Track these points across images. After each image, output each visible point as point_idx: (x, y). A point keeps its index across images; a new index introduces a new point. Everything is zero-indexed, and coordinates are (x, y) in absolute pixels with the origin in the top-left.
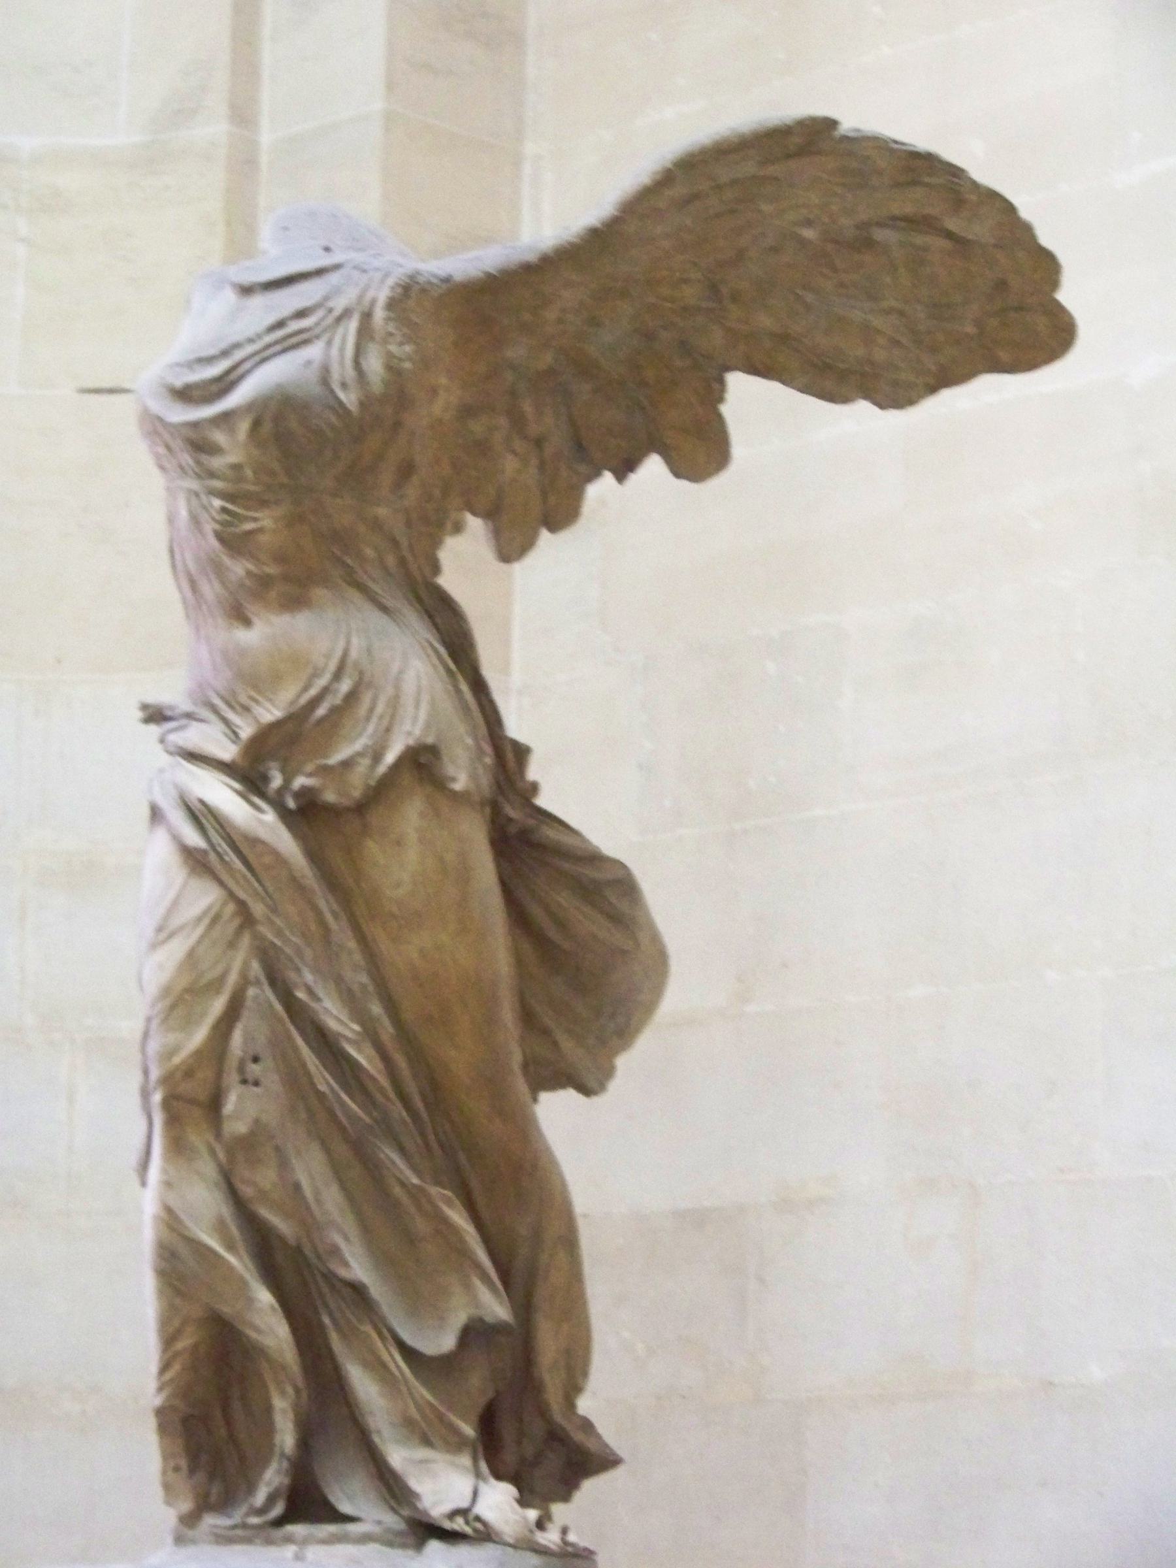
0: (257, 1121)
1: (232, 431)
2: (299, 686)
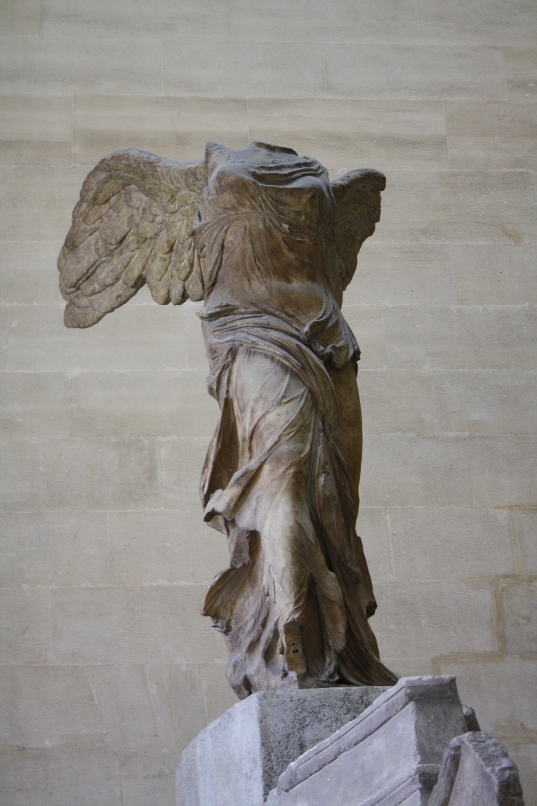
0: (330, 491)
1: (300, 198)
2: (323, 311)
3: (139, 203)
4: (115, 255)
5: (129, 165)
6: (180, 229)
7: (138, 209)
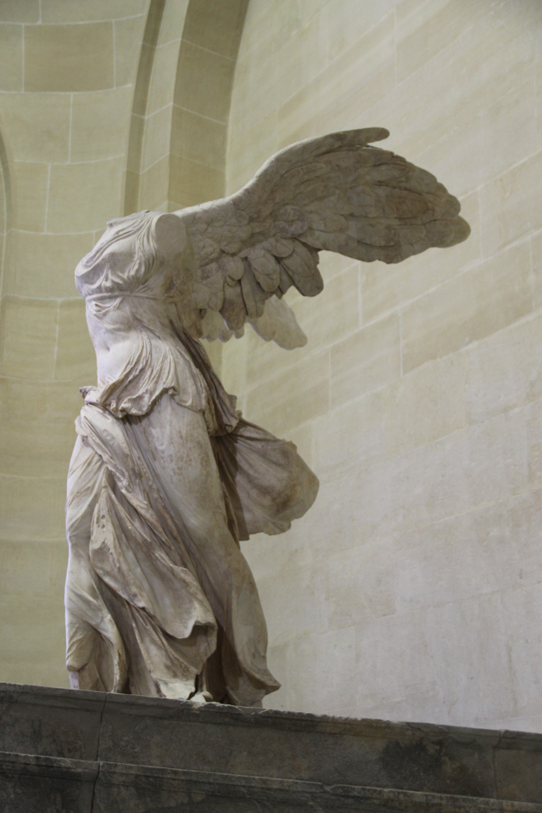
0: (104, 543)
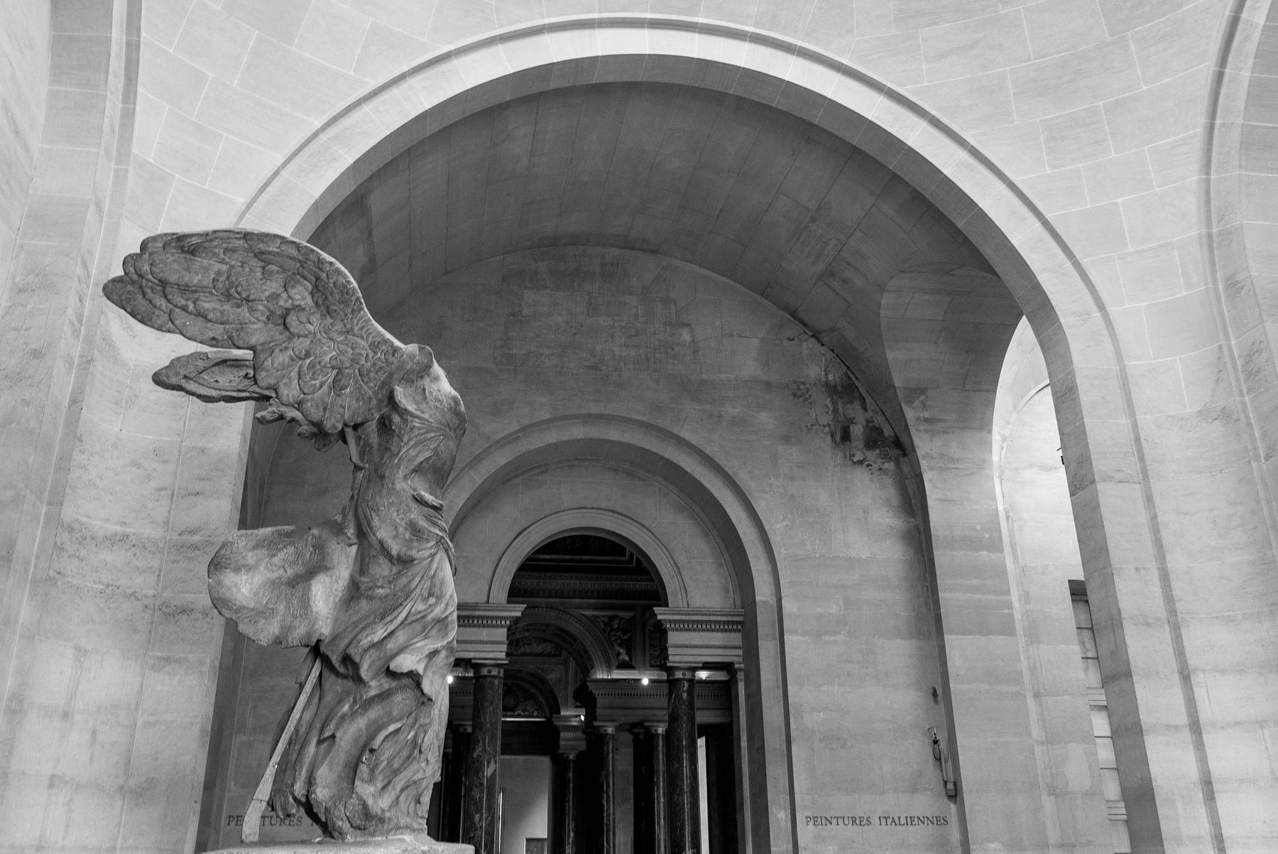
3: (298, 297)
4: (232, 302)
5: (345, 287)
6: (325, 353)
7: (290, 297)
